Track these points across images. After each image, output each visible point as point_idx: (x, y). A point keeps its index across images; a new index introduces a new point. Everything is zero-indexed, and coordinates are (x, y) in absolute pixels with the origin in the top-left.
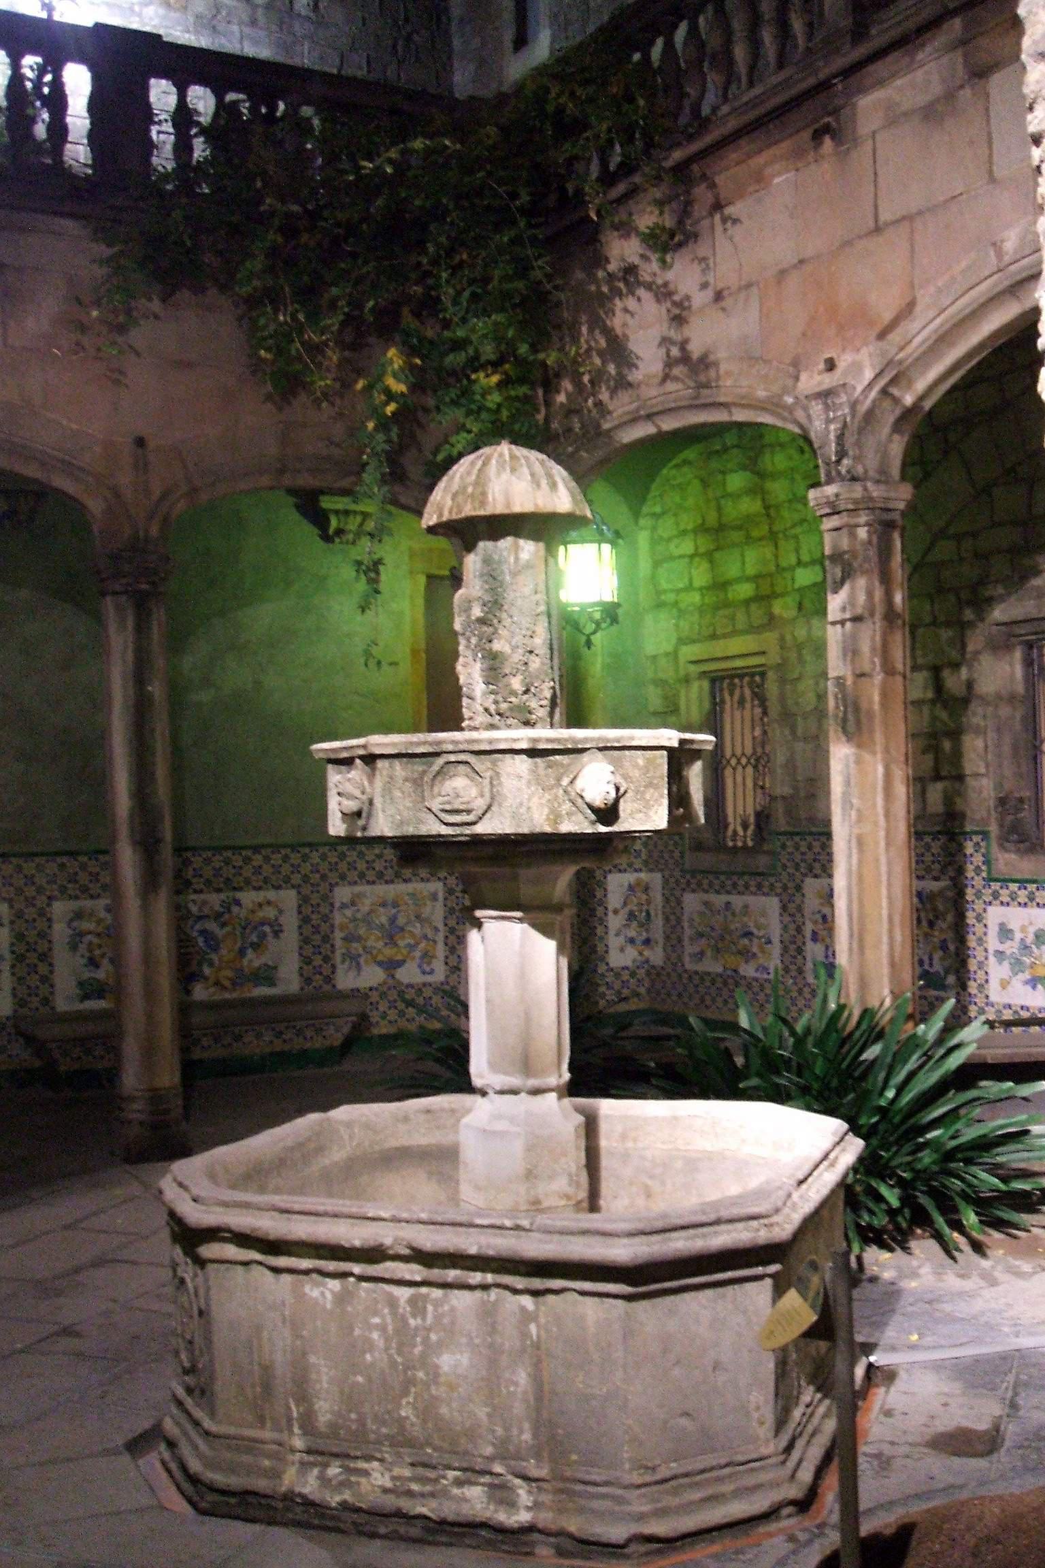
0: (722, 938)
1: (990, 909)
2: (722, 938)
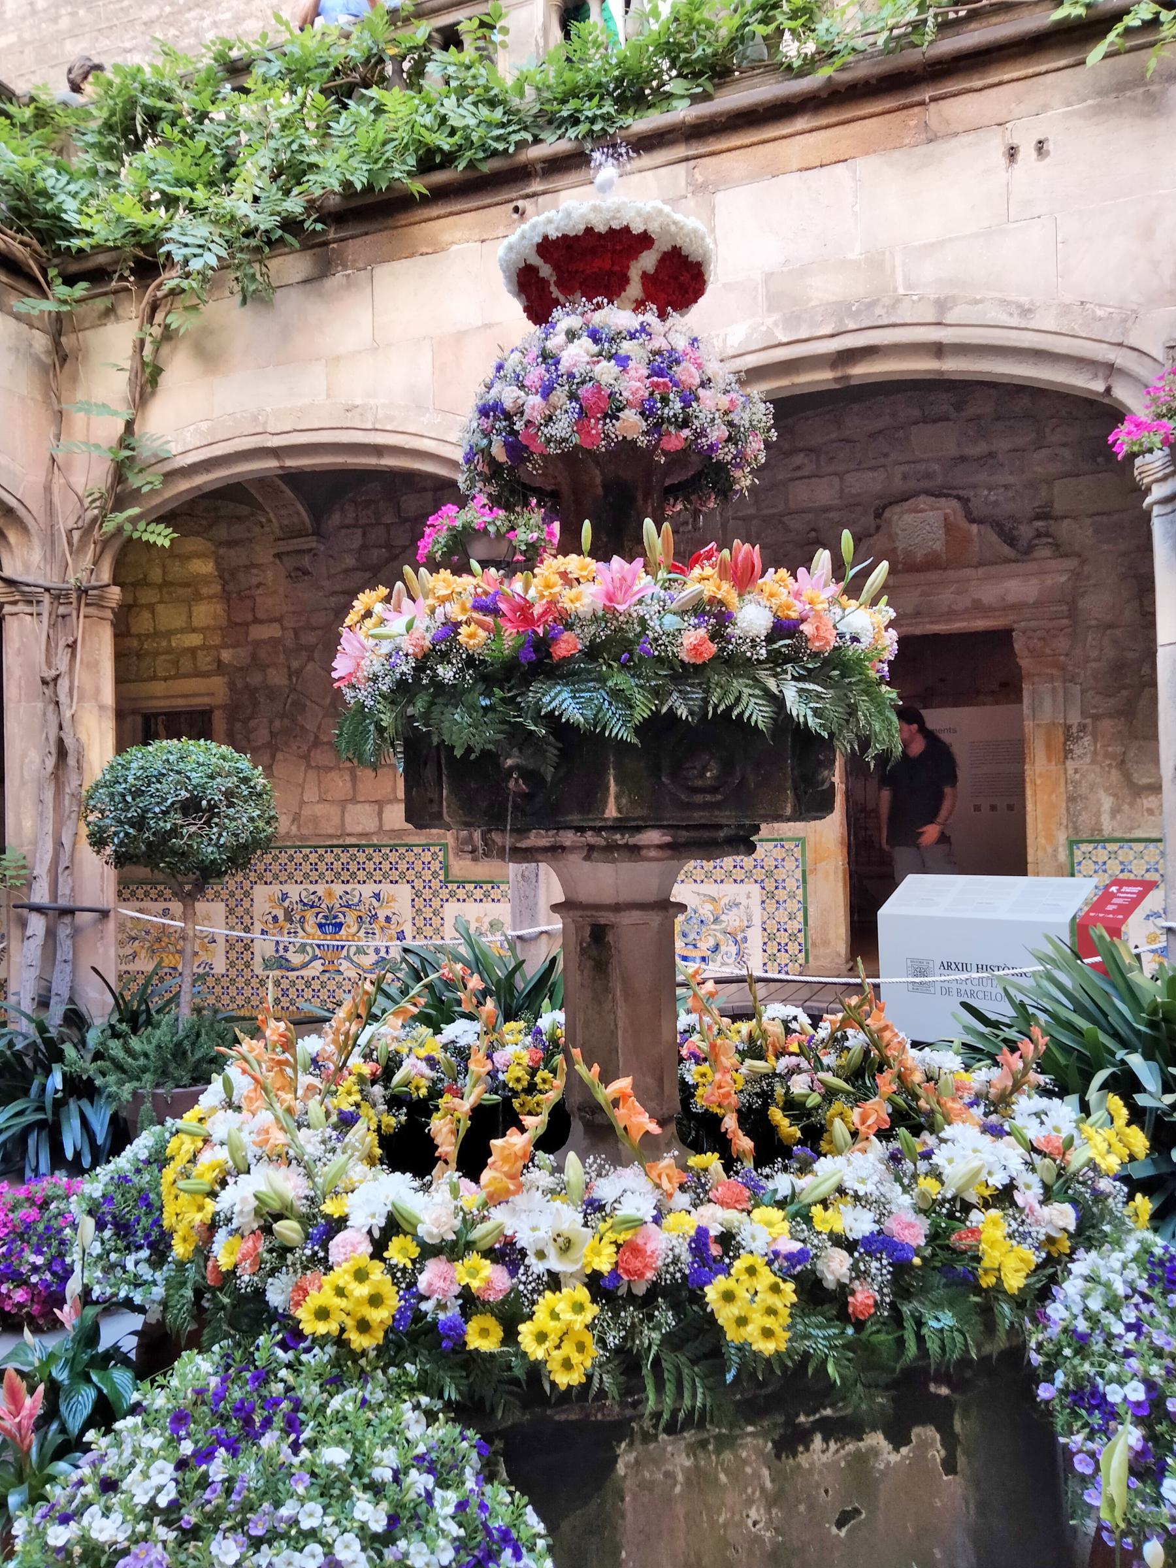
0: (159, 940)
1: (446, 905)
2: (159, 940)
